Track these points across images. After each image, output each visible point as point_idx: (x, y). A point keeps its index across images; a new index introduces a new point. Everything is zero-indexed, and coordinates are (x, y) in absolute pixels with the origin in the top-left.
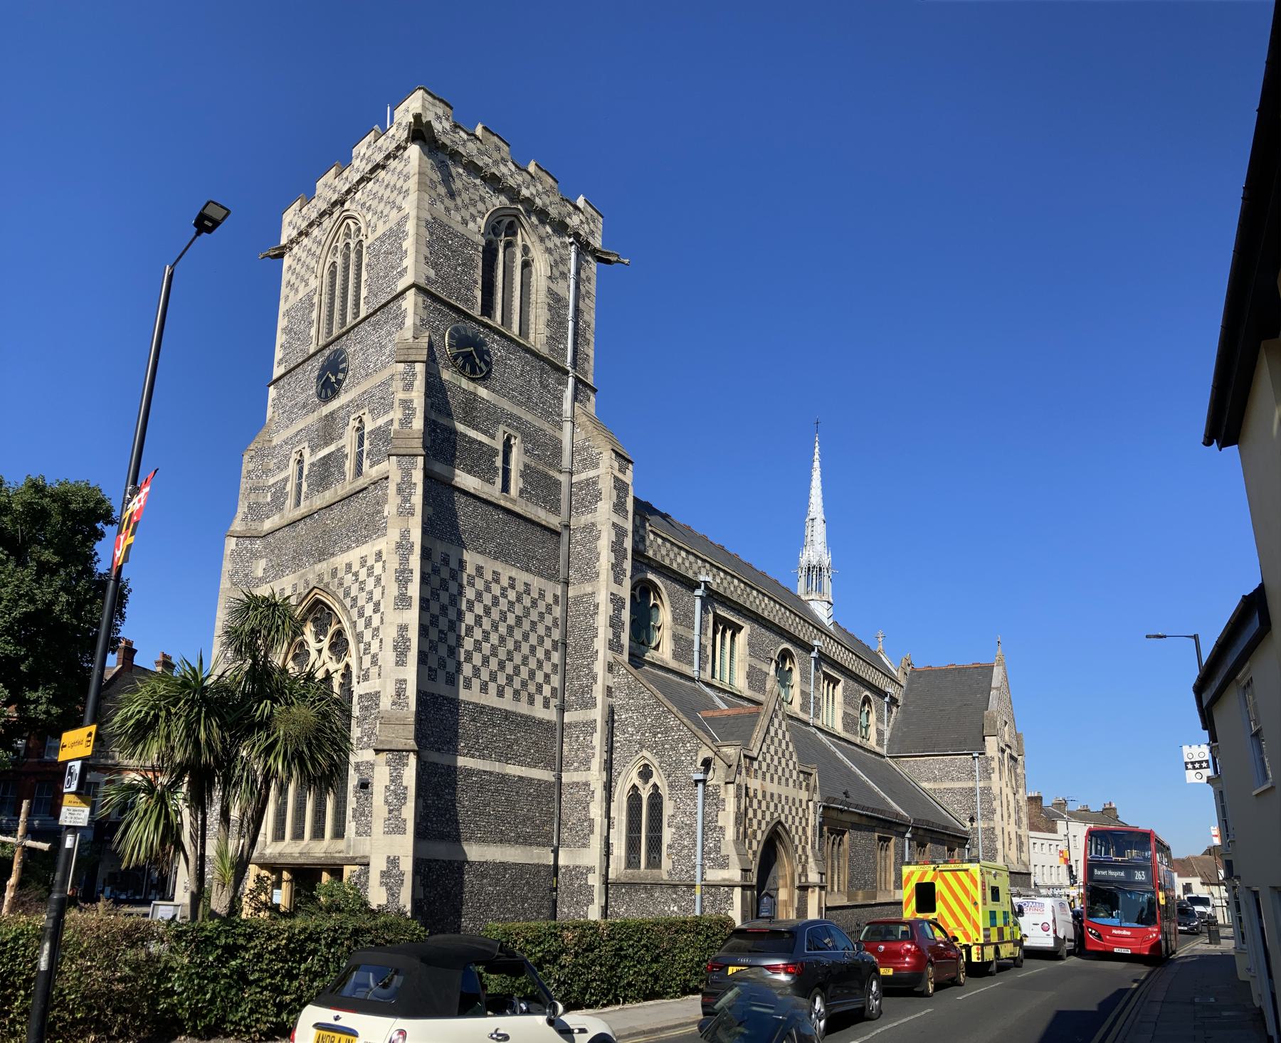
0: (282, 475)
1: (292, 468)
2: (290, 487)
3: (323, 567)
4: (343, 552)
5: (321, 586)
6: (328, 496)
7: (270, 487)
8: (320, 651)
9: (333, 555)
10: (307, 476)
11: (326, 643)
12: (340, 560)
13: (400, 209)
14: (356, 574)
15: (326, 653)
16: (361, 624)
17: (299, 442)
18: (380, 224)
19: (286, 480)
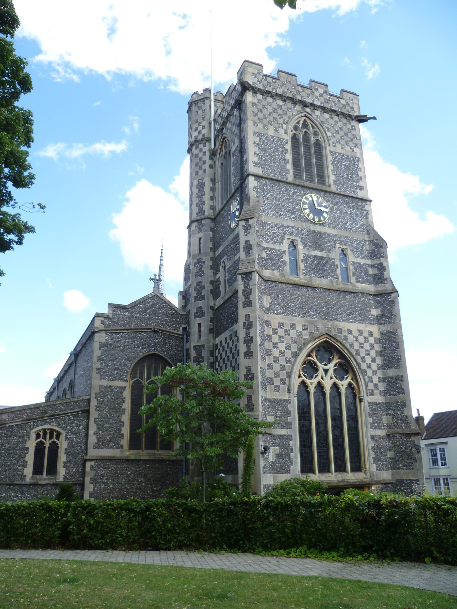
0: (277, 247)
1: (285, 246)
2: (286, 258)
3: (330, 324)
4: (344, 321)
5: (331, 334)
6: (324, 282)
7: (264, 248)
8: (326, 371)
9: (336, 320)
10: (304, 261)
11: (331, 366)
12: (344, 326)
13: (353, 151)
14: (356, 338)
15: (331, 373)
16: (364, 366)
17: (291, 233)
18: (338, 146)
19: (283, 252)
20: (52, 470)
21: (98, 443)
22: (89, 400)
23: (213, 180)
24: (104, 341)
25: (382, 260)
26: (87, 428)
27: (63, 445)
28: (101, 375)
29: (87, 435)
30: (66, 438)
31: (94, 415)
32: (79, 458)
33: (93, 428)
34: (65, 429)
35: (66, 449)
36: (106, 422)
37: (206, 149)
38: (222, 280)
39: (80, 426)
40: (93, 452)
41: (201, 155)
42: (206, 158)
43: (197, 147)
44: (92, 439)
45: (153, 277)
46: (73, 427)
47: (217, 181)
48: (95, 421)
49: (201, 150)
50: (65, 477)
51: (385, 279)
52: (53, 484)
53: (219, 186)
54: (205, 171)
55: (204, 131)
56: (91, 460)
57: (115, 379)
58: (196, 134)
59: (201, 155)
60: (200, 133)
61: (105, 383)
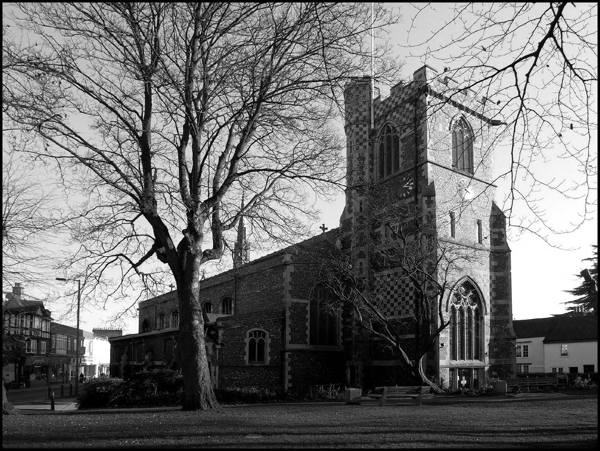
20: (261, 357)
21: (292, 340)
22: (284, 313)
23: (372, 156)
24: (293, 271)
25: (502, 230)
26: (283, 330)
27: (268, 341)
28: (292, 295)
29: (283, 335)
30: (270, 337)
31: (288, 322)
32: (279, 350)
33: (288, 331)
34: (268, 331)
35: (270, 344)
36: (297, 327)
37: (366, 129)
38: (383, 233)
39: (278, 329)
40: (289, 346)
41: (361, 133)
42: (366, 136)
43: (357, 126)
44: (288, 338)
45: (322, 226)
46: (274, 329)
47: (375, 157)
48: (290, 326)
49: (361, 129)
50: (270, 362)
51: (503, 242)
52: (263, 366)
53: (376, 161)
54: (365, 147)
55: (364, 114)
56: (288, 351)
57: (301, 298)
58: (357, 115)
59: (361, 133)
60: (361, 114)
61: (295, 300)
